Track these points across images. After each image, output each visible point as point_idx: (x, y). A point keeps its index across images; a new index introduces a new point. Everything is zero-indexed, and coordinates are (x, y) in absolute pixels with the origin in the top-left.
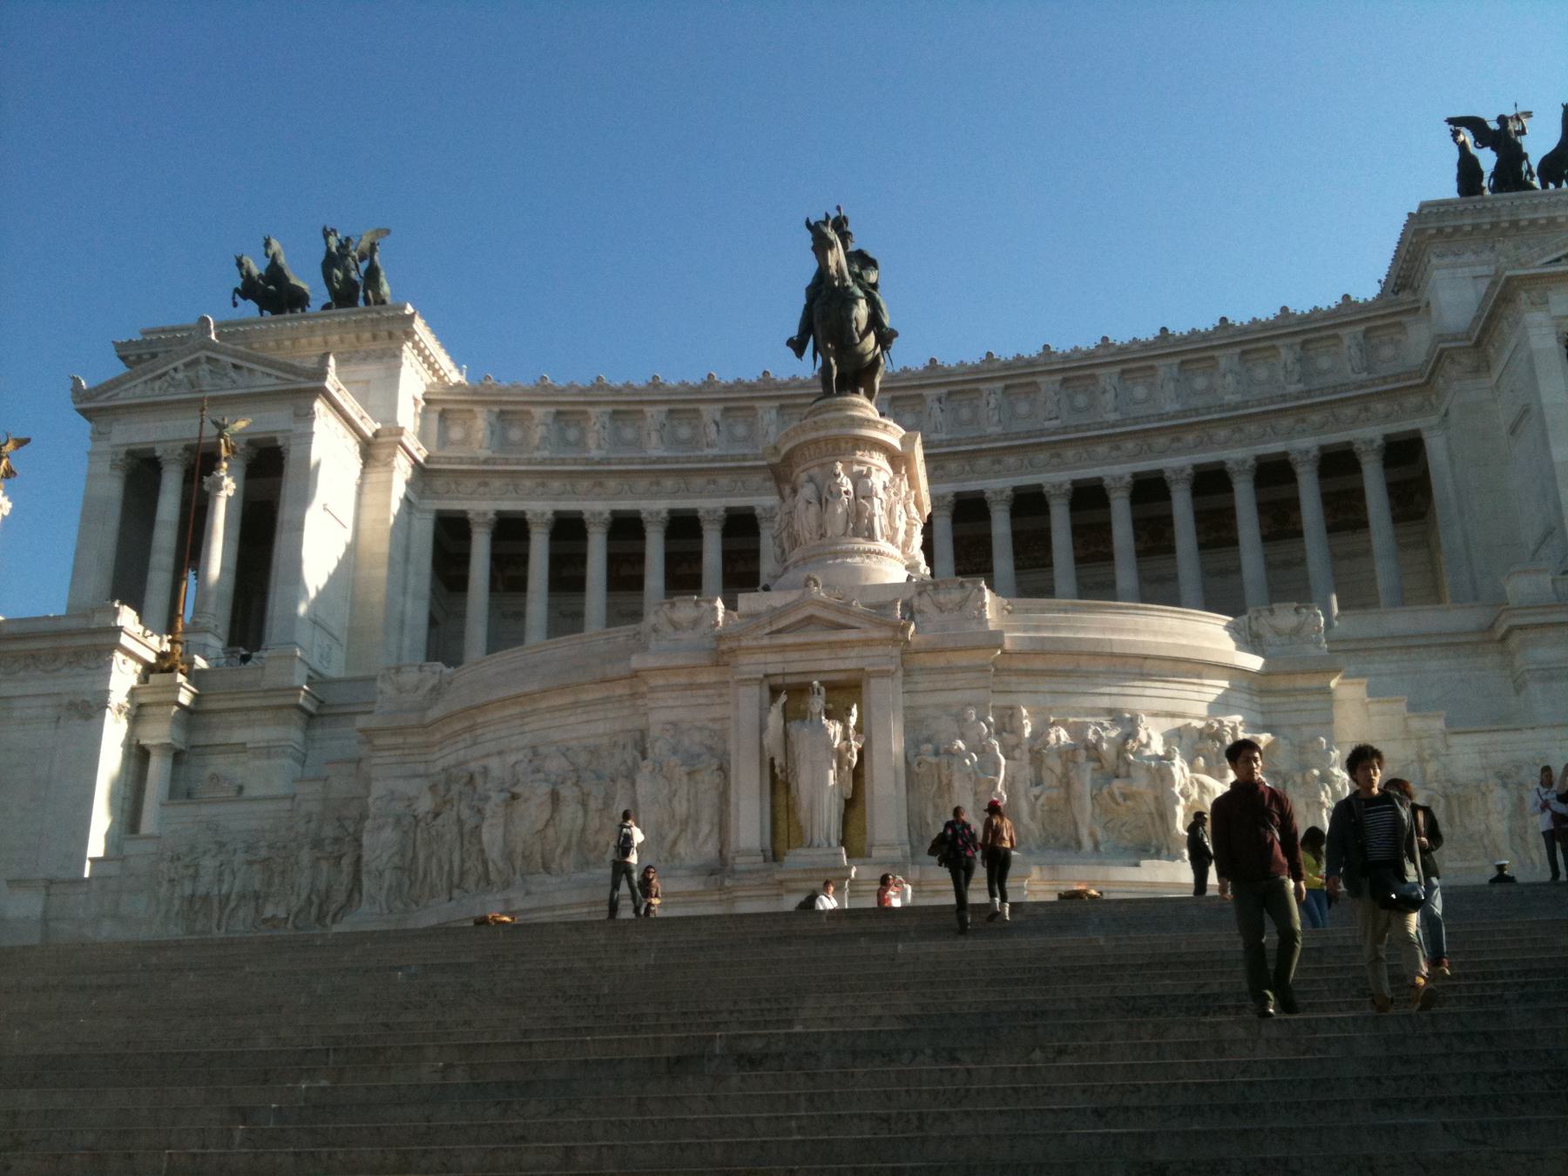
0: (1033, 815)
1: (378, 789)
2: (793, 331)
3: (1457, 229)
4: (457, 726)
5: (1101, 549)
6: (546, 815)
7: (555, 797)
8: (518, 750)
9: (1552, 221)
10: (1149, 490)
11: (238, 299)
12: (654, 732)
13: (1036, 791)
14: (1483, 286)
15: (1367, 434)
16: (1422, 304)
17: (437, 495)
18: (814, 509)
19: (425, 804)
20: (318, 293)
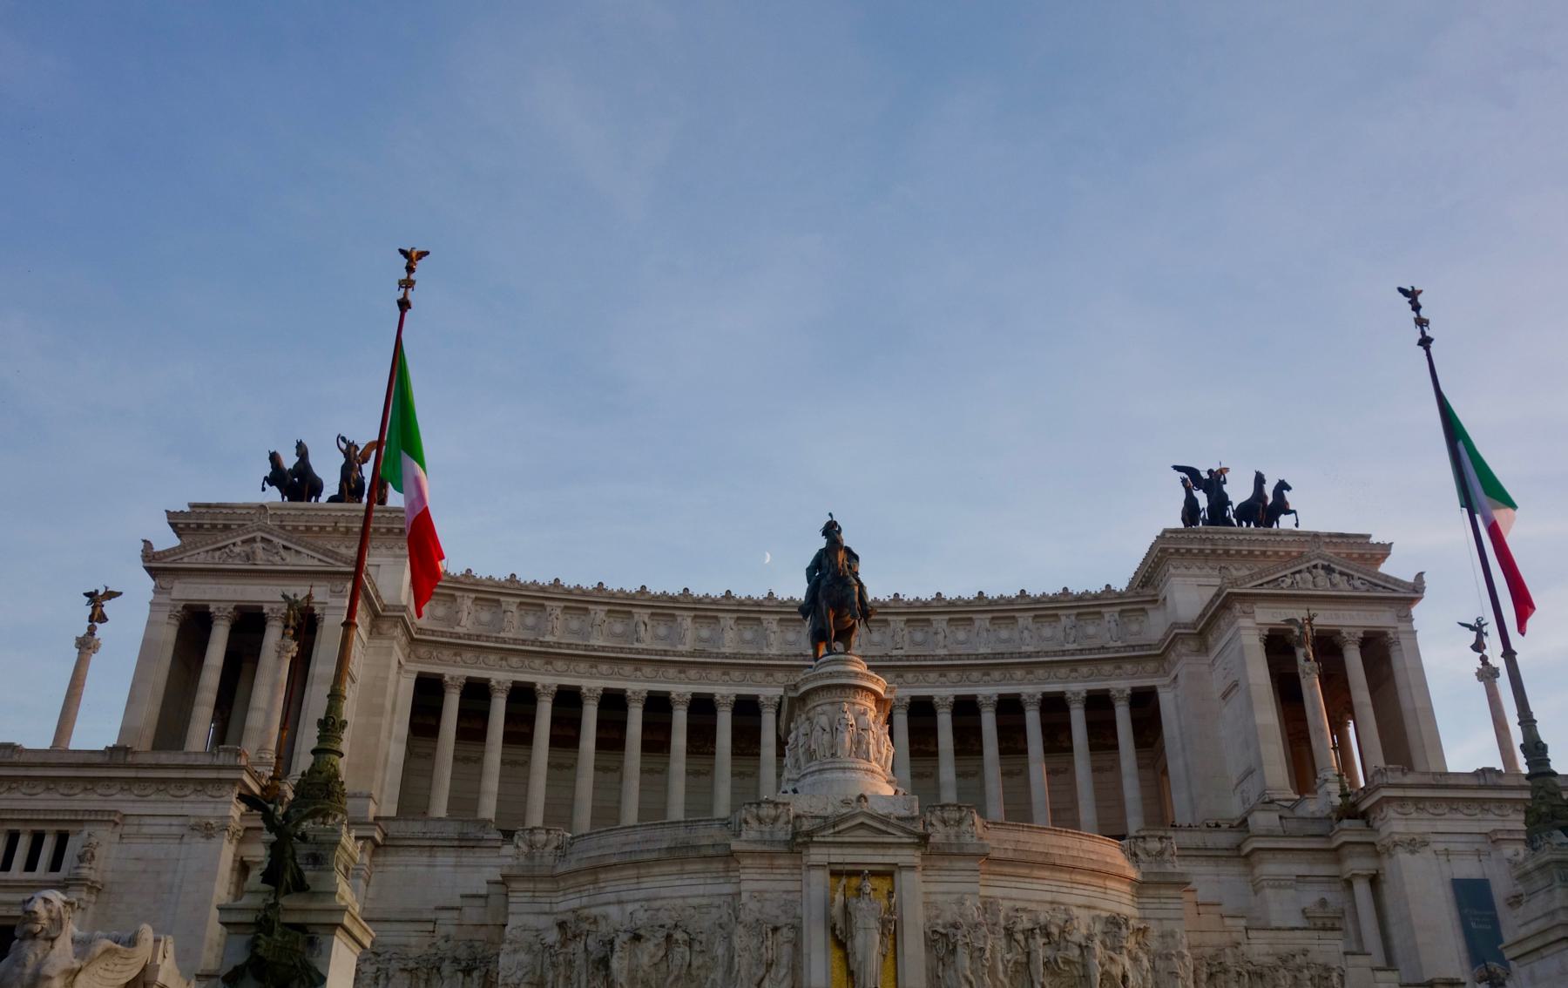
0: (1005, 972)
1: (513, 921)
3: (1189, 551)
4: (582, 880)
5: (923, 747)
6: (661, 953)
7: (669, 937)
9: (1251, 552)
10: (966, 709)
12: (745, 897)
13: (1008, 956)
15: (1120, 685)
16: (1161, 598)
17: (419, 659)
18: (827, 737)
19: (553, 936)
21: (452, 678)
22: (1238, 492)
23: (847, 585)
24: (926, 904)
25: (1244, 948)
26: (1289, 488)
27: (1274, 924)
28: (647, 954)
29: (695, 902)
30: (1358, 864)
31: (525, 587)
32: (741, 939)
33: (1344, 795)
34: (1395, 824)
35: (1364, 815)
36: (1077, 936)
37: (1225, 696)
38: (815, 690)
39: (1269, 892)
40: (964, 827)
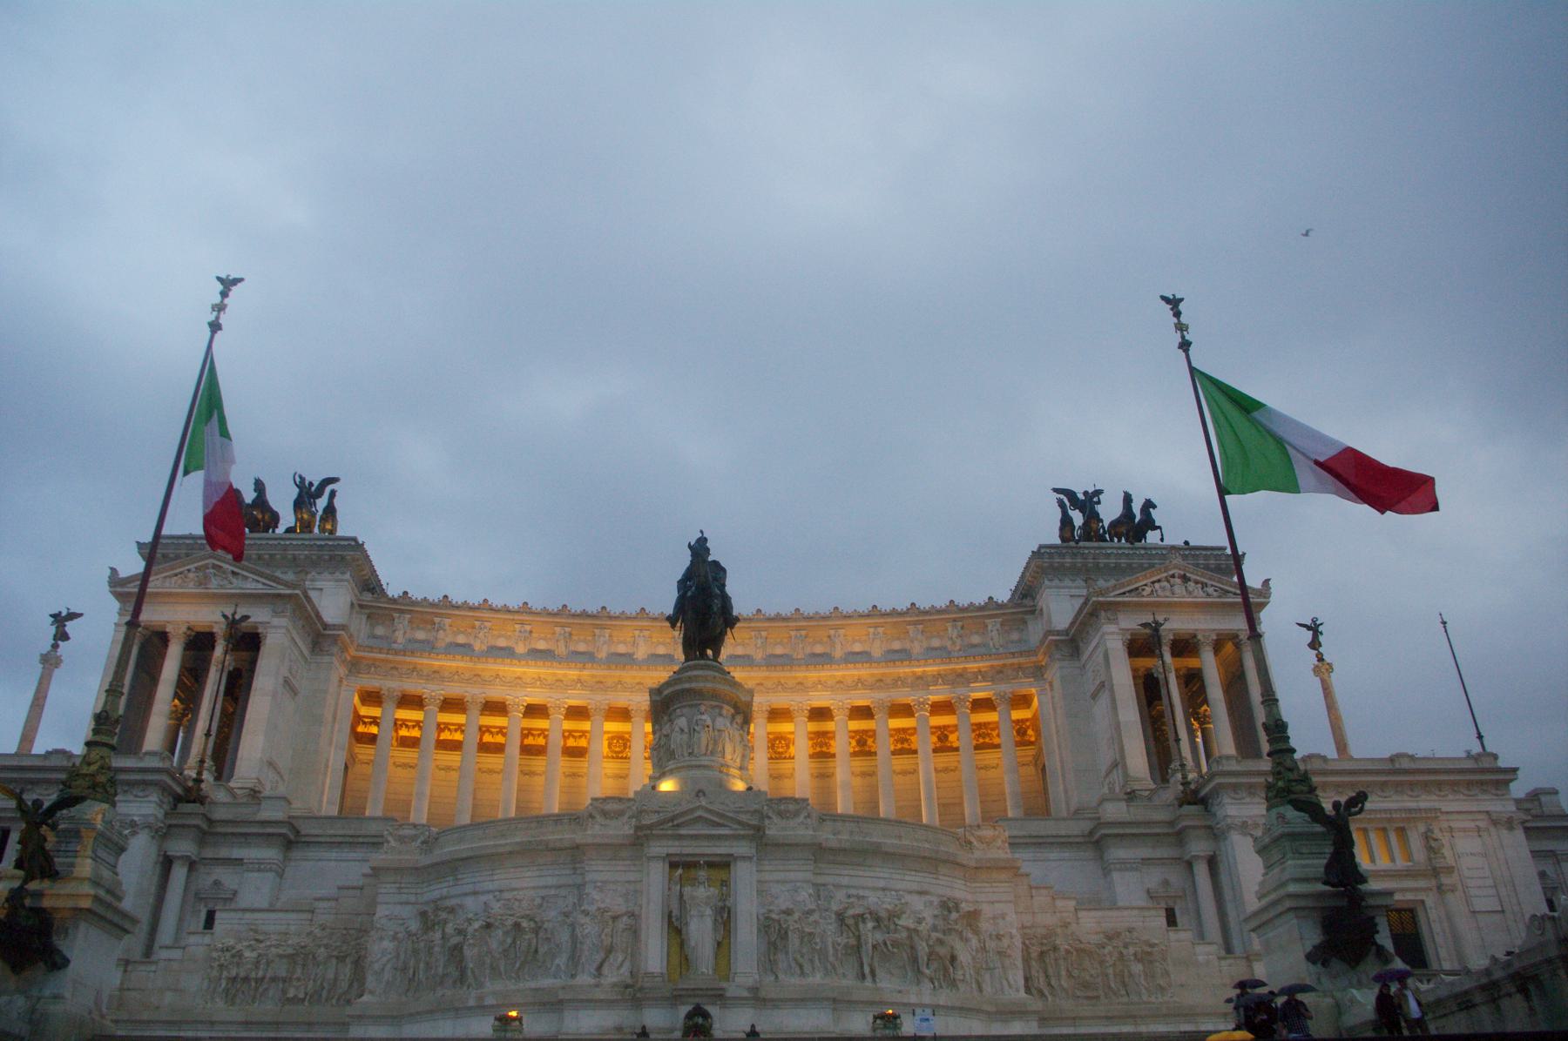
1: (381, 911)
2: (670, 611)
6: (509, 940)
7: (517, 925)
8: (489, 892)
9: (1117, 566)
14: (1078, 603)
18: (685, 737)
19: (414, 926)
20: (287, 519)
22: (1109, 511)
25: (1074, 927)
26: (1154, 507)
27: (1120, 904)
28: (496, 941)
29: (543, 892)
30: (1199, 847)
33: (1185, 783)
39: (1116, 875)
40: (801, 818)
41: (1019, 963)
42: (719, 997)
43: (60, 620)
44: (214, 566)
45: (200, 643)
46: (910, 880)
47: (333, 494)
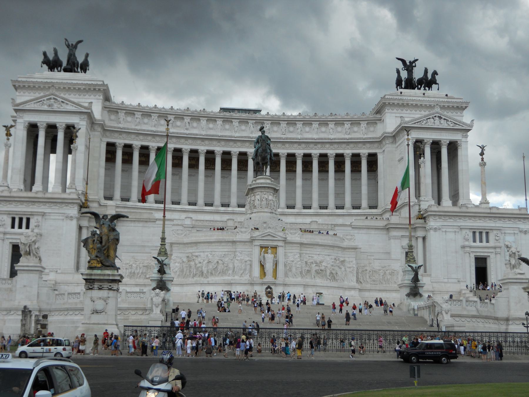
3: (394, 103)
4: (192, 245)
7: (218, 262)
11: (43, 65)
15: (364, 152)
16: (382, 119)
17: (107, 137)
18: (259, 202)
19: (185, 260)
20: (65, 64)
21: (119, 144)
23: (266, 152)
24: (285, 255)
26: (437, 74)
29: (224, 253)
30: (420, 233)
31: (144, 108)
32: (237, 263)
33: (420, 212)
34: (432, 223)
35: (424, 218)
36: (323, 264)
37: (399, 161)
38: (257, 187)
40: (297, 235)
41: (355, 275)
42: (275, 284)
43: (8, 128)
44: (54, 99)
45: (52, 129)
46: (327, 252)
47: (87, 55)
